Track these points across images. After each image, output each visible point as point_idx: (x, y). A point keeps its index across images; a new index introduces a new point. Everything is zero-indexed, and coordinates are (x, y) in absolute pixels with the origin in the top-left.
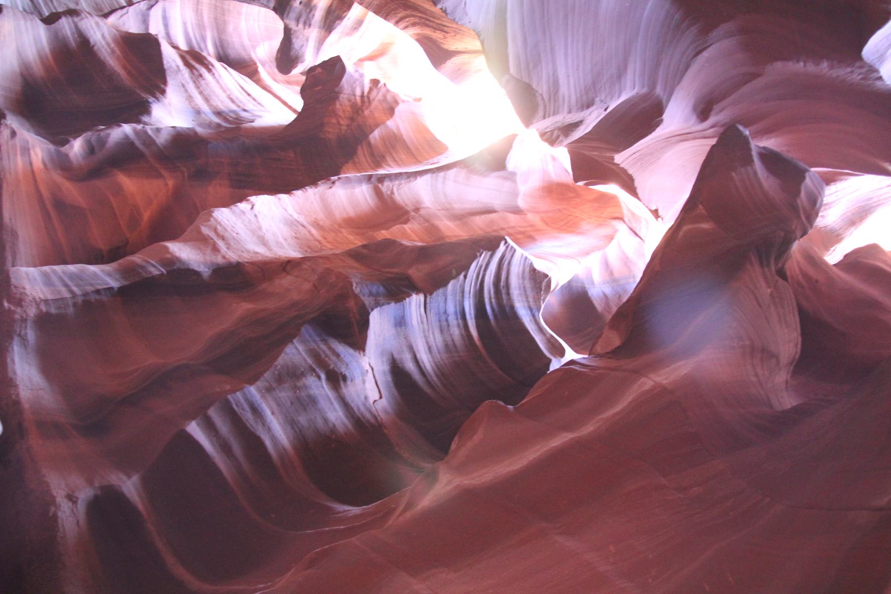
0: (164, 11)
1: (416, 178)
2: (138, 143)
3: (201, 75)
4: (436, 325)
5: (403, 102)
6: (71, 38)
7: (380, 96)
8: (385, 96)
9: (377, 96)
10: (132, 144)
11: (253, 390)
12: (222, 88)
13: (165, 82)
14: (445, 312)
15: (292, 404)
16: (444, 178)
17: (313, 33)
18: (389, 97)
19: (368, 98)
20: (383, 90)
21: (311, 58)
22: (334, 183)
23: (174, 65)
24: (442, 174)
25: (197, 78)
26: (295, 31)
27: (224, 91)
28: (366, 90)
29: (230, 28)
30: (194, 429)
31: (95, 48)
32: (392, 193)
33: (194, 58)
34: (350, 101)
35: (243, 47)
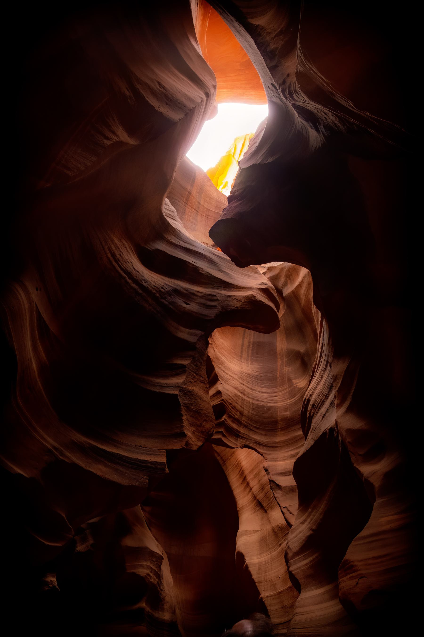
3: (313, 405)
6: (311, 559)
12: (320, 381)
13: (324, 434)
25: (317, 407)
26: (223, 308)
29: (288, 414)
31: (314, 527)
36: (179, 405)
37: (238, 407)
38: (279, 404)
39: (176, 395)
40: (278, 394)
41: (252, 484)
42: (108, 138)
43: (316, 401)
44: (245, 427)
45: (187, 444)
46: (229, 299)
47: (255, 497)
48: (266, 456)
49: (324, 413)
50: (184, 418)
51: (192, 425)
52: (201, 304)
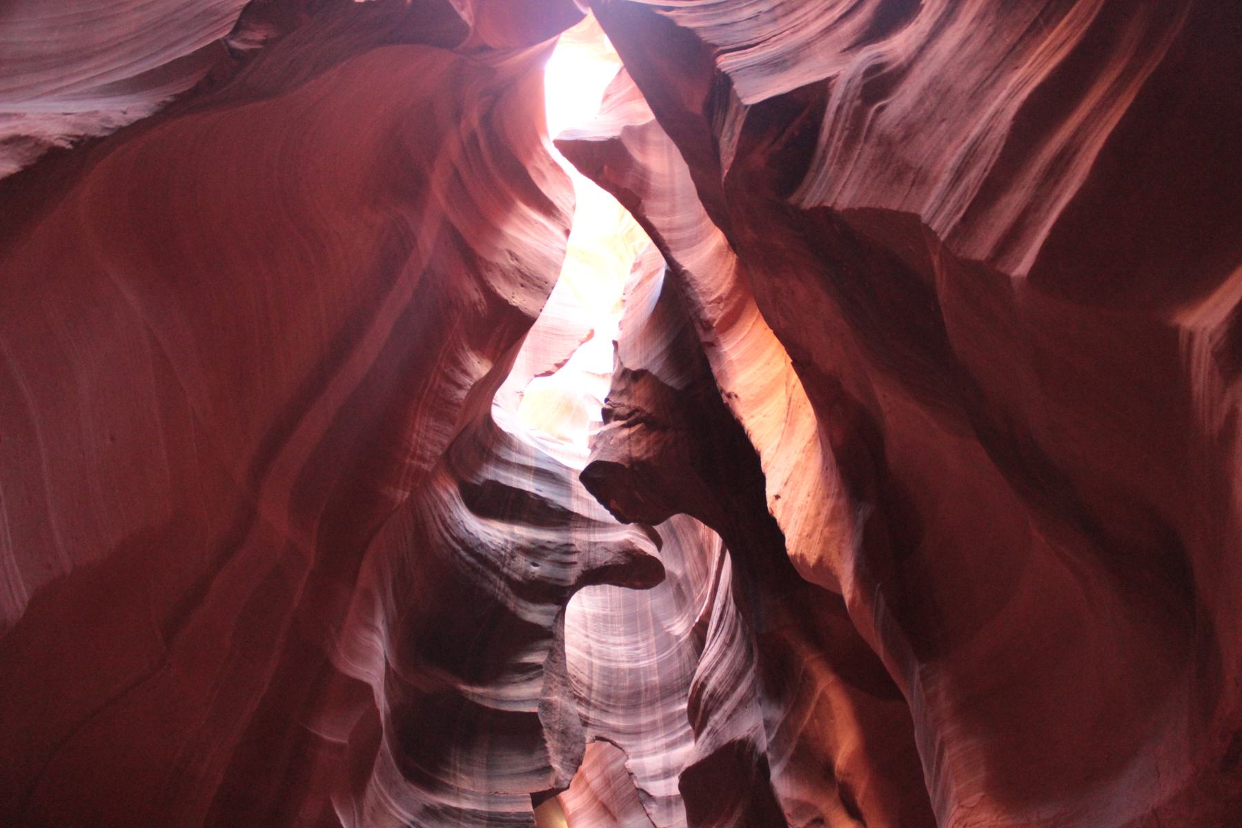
0: (654, 778)
1: (686, 271)
2: (790, 751)
3: (711, 696)
4: (783, 24)
5: (621, 364)
7: (624, 400)
8: (622, 393)
9: (625, 404)
10: (793, 759)
11: (925, 212)
13: (731, 744)
14: (756, 17)
15: (943, 120)
16: (670, 230)
17: (580, 537)
18: (622, 387)
19: (630, 415)
20: (613, 400)
21: (627, 534)
22: (729, 396)
23: (708, 741)
24: (665, 236)
25: (717, 700)
27: (724, 655)
28: (619, 423)
29: (655, 679)
30: (1022, 267)
32: (719, 300)
33: (698, 716)
34: (638, 441)
35: (679, 652)
36: (541, 727)
37: (585, 680)
38: (643, 664)
39: (535, 715)
40: (641, 645)
41: (588, 776)
42: (460, 387)
43: (715, 690)
44: (595, 707)
45: (557, 782)
46: (593, 549)
47: (595, 798)
48: (628, 750)
49: (729, 713)
50: (548, 745)
51: (557, 752)
52: (554, 562)
